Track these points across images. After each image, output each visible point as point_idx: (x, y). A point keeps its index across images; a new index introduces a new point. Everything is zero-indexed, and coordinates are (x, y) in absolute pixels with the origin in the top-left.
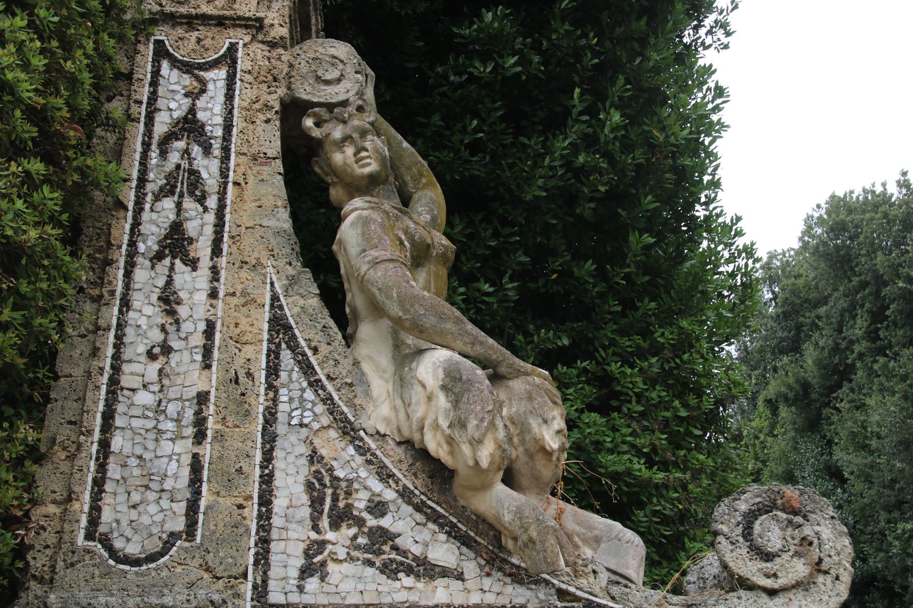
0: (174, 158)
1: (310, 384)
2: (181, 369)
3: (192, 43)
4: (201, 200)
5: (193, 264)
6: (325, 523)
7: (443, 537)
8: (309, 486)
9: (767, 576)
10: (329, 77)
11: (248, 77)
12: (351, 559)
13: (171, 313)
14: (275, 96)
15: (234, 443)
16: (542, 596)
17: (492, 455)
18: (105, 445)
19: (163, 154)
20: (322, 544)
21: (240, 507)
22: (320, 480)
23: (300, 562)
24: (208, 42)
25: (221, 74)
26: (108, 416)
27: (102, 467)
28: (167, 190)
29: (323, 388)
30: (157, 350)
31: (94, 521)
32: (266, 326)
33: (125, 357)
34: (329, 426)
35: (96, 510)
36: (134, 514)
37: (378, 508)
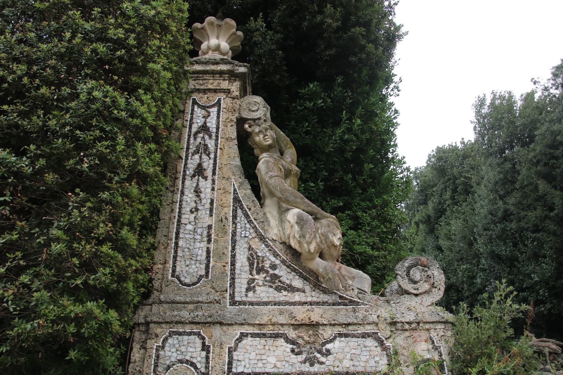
0: (199, 140)
1: (248, 222)
2: (202, 217)
4: (208, 155)
5: (206, 178)
6: (254, 272)
7: (297, 277)
8: (249, 259)
9: (415, 289)
10: (253, 109)
11: (225, 110)
12: (264, 285)
13: (198, 196)
14: (234, 117)
16: (333, 298)
17: (315, 248)
18: (176, 244)
19: (195, 139)
20: (254, 280)
21: (224, 266)
22: (252, 257)
23: (246, 286)
24: (211, 98)
25: (215, 109)
26: (177, 234)
27: (176, 252)
28: (197, 152)
29: (253, 223)
30: (193, 210)
31: (174, 271)
32: (232, 201)
33: (183, 212)
34: (255, 237)
35: (174, 266)
36: (187, 269)
37: (274, 267)
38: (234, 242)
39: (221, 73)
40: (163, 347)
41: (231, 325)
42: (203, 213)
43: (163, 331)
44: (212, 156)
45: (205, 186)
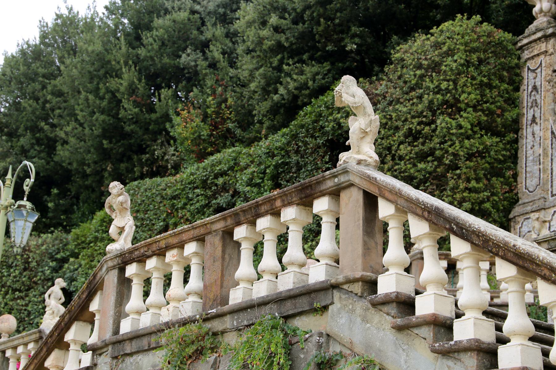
0: (533, 98)
3: (533, 64)
4: (537, 107)
5: (537, 124)
11: (545, 68)
13: (534, 137)
15: (546, 163)
24: (537, 62)
26: (526, 164)
27: (526, 175)
28: (532, 107)
35: (526, 183)
38: (552, 160)
39: (539, 39)
40: (522, 227)
41: (549, 208)
42: (536, 147)
43: (520, 219)
44: (539, 107)
45: (536, 128)
